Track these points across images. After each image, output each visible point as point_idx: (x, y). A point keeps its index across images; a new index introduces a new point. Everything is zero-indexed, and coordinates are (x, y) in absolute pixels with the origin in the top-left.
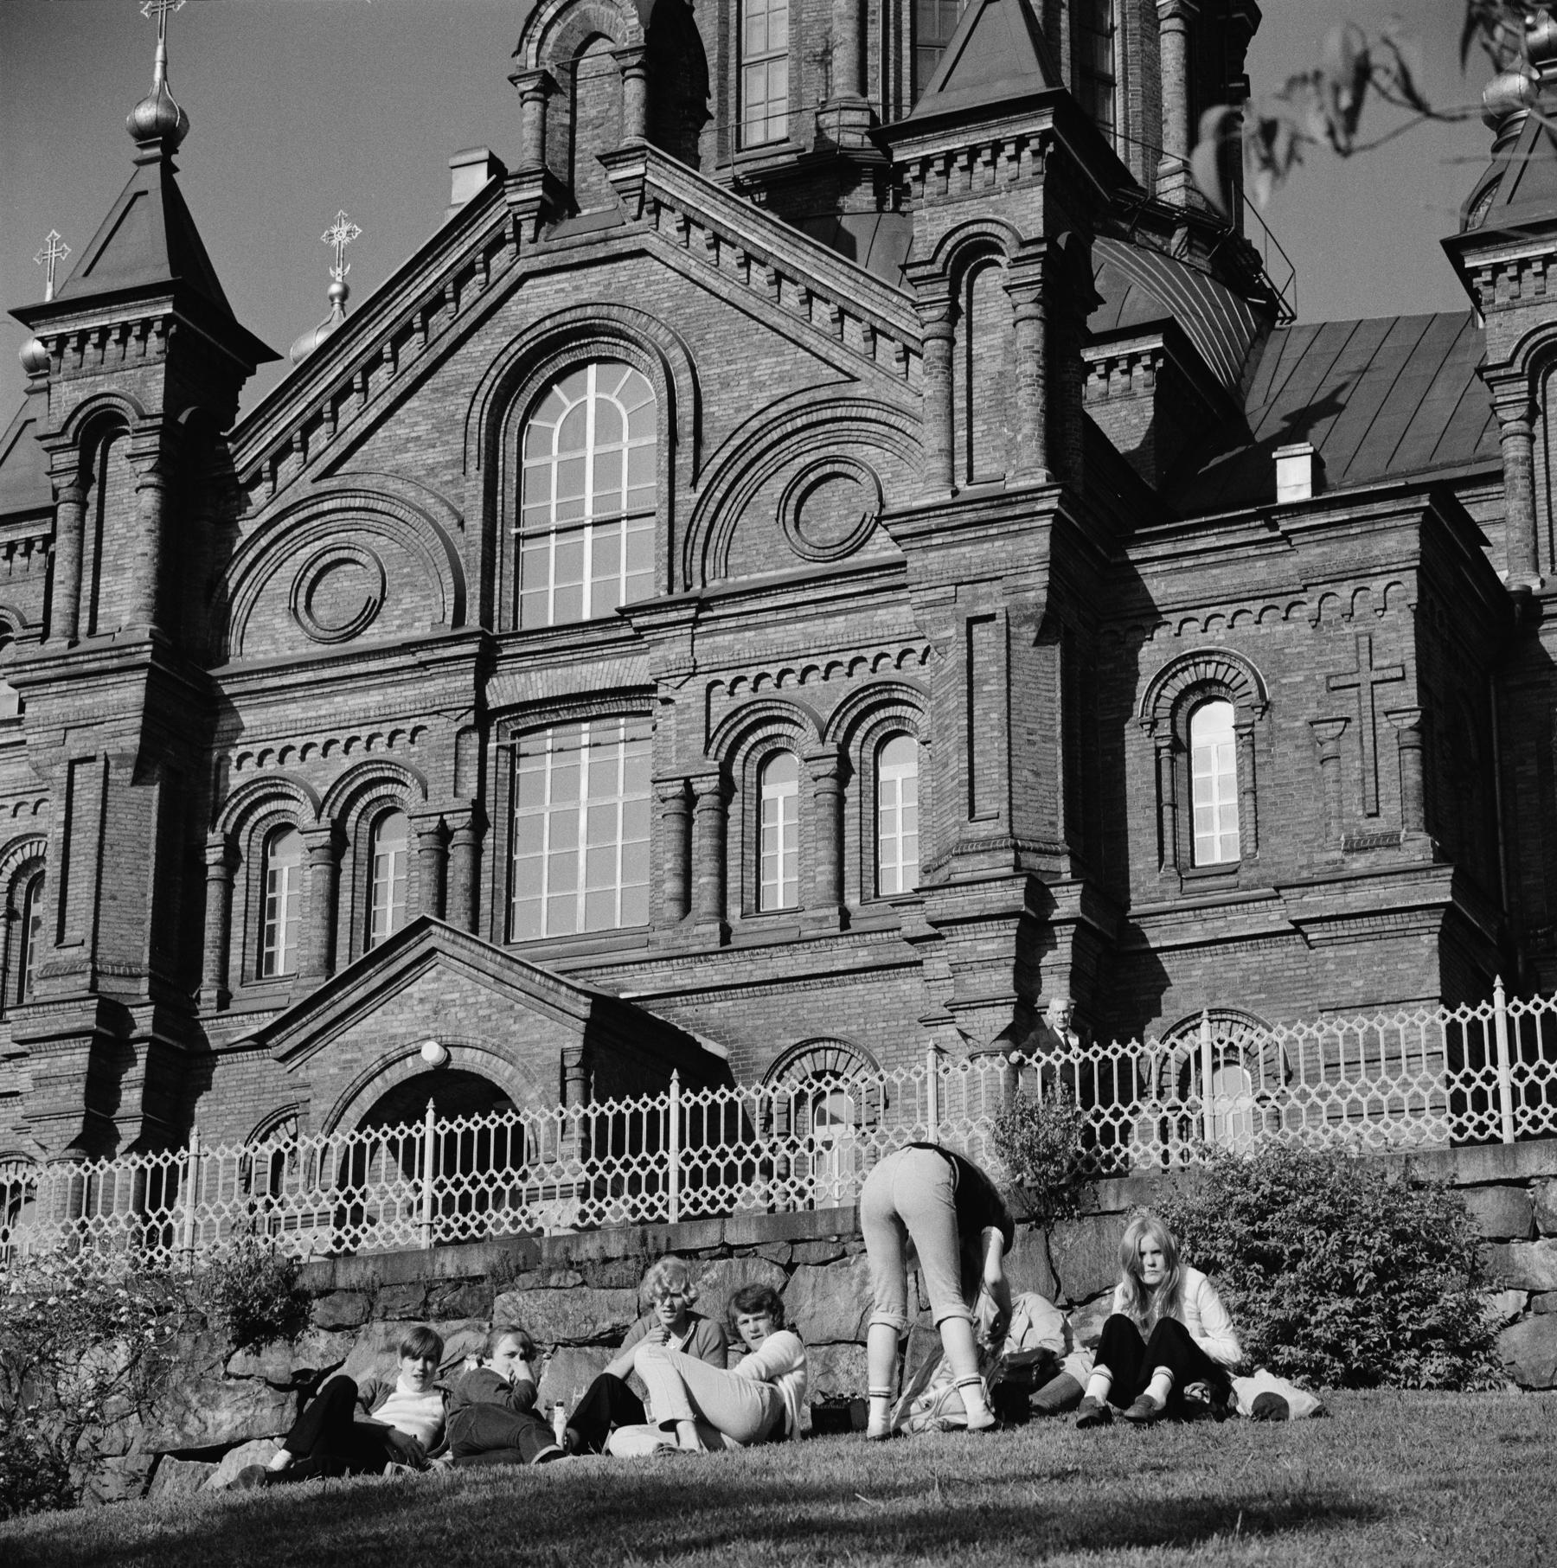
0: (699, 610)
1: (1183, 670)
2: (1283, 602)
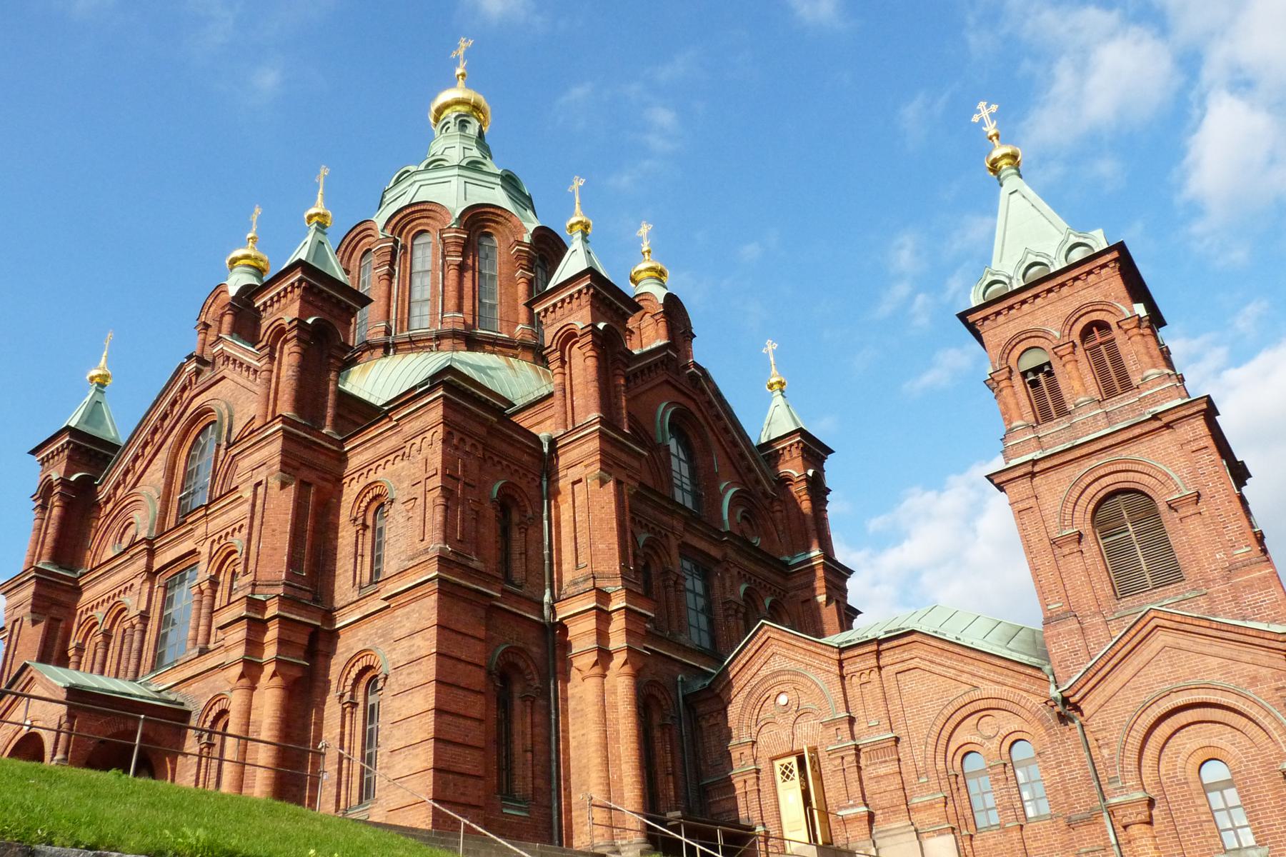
0: (207, 510)
1: (368, 492)
2: (400, 453)
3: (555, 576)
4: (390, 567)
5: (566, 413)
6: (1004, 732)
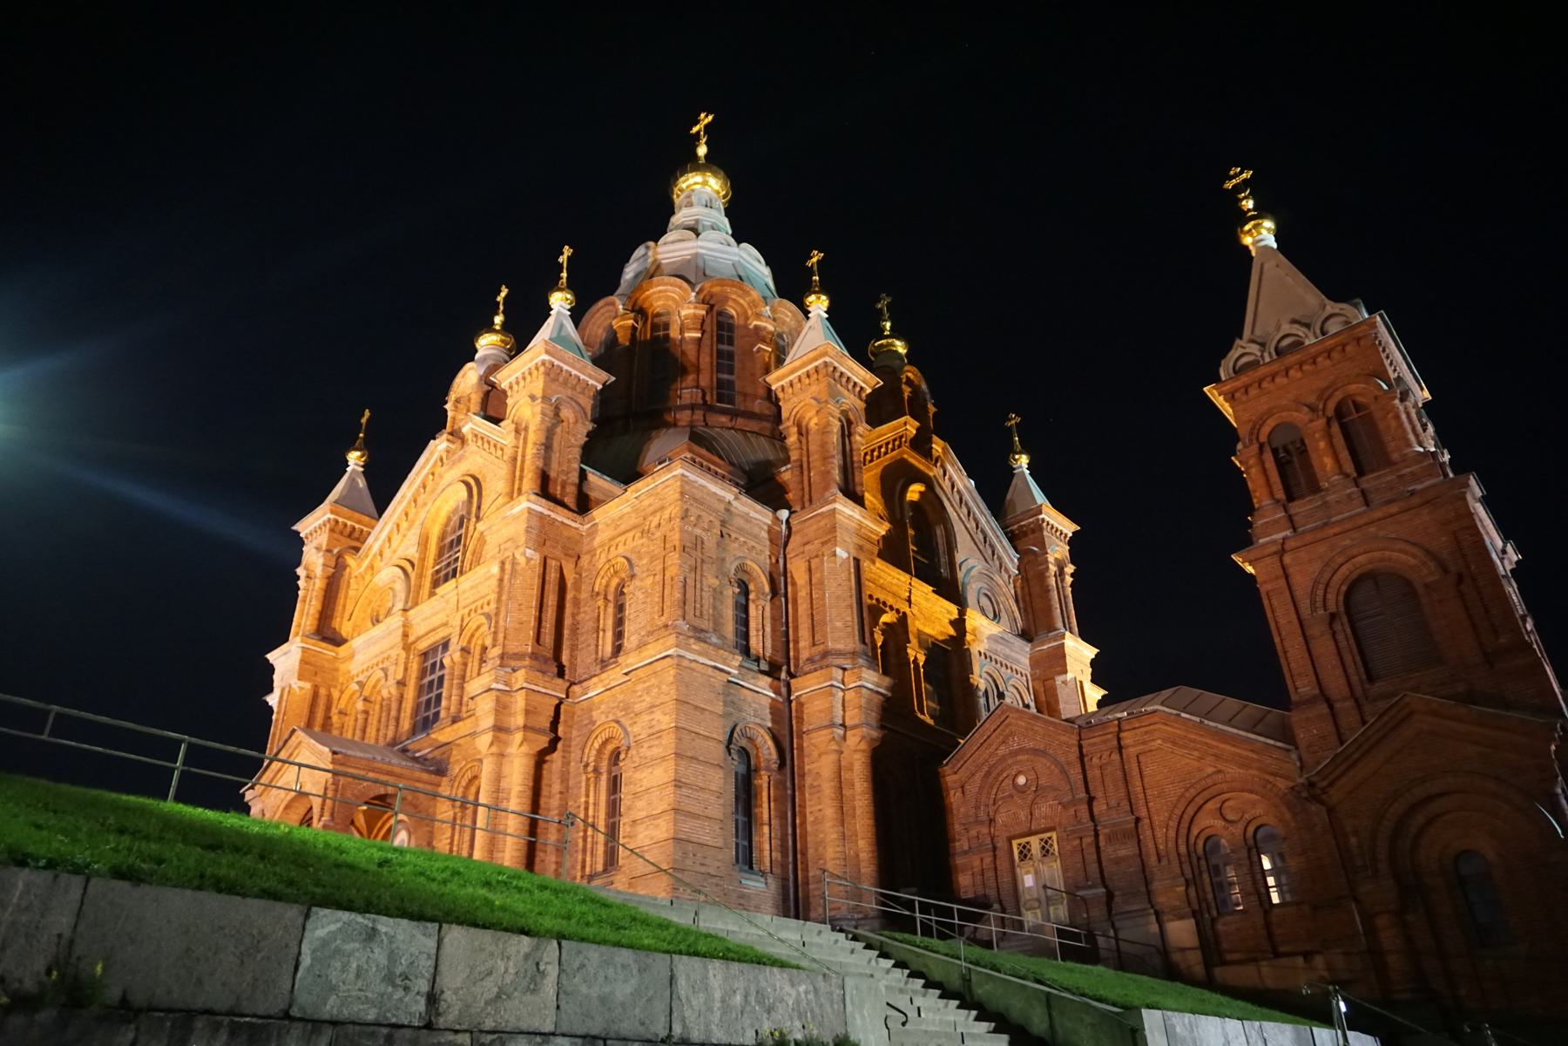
3: (792, 654)
4: (630, 641)
5: (803, 489)
6: (1247, 816)
